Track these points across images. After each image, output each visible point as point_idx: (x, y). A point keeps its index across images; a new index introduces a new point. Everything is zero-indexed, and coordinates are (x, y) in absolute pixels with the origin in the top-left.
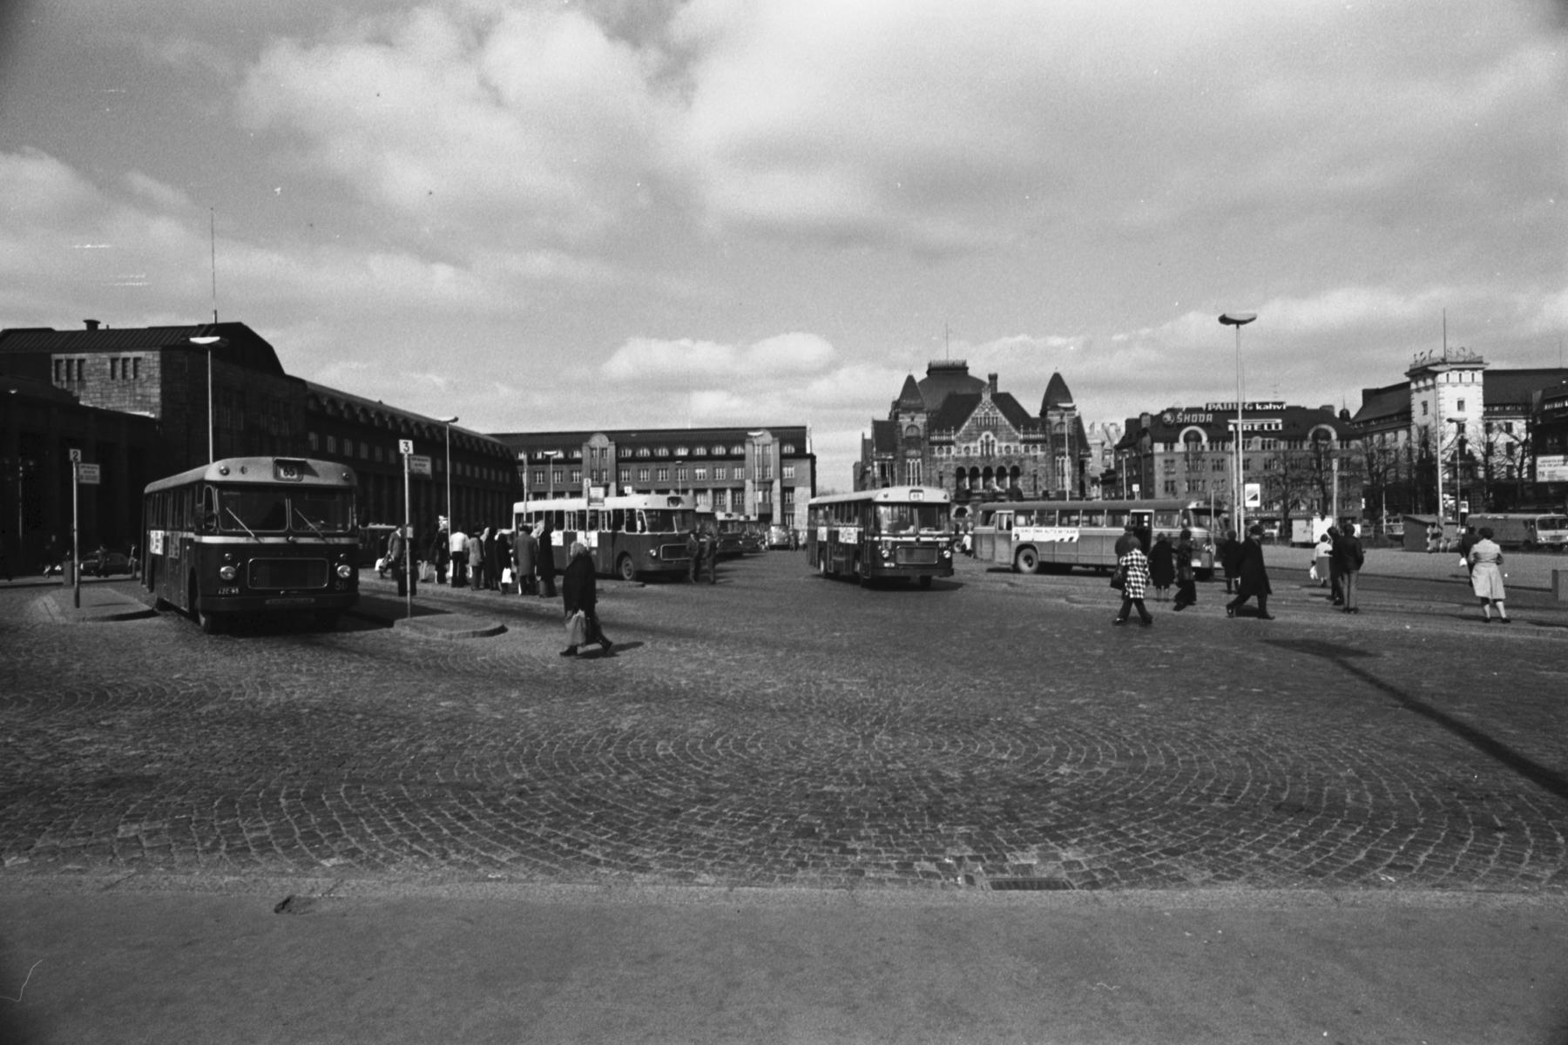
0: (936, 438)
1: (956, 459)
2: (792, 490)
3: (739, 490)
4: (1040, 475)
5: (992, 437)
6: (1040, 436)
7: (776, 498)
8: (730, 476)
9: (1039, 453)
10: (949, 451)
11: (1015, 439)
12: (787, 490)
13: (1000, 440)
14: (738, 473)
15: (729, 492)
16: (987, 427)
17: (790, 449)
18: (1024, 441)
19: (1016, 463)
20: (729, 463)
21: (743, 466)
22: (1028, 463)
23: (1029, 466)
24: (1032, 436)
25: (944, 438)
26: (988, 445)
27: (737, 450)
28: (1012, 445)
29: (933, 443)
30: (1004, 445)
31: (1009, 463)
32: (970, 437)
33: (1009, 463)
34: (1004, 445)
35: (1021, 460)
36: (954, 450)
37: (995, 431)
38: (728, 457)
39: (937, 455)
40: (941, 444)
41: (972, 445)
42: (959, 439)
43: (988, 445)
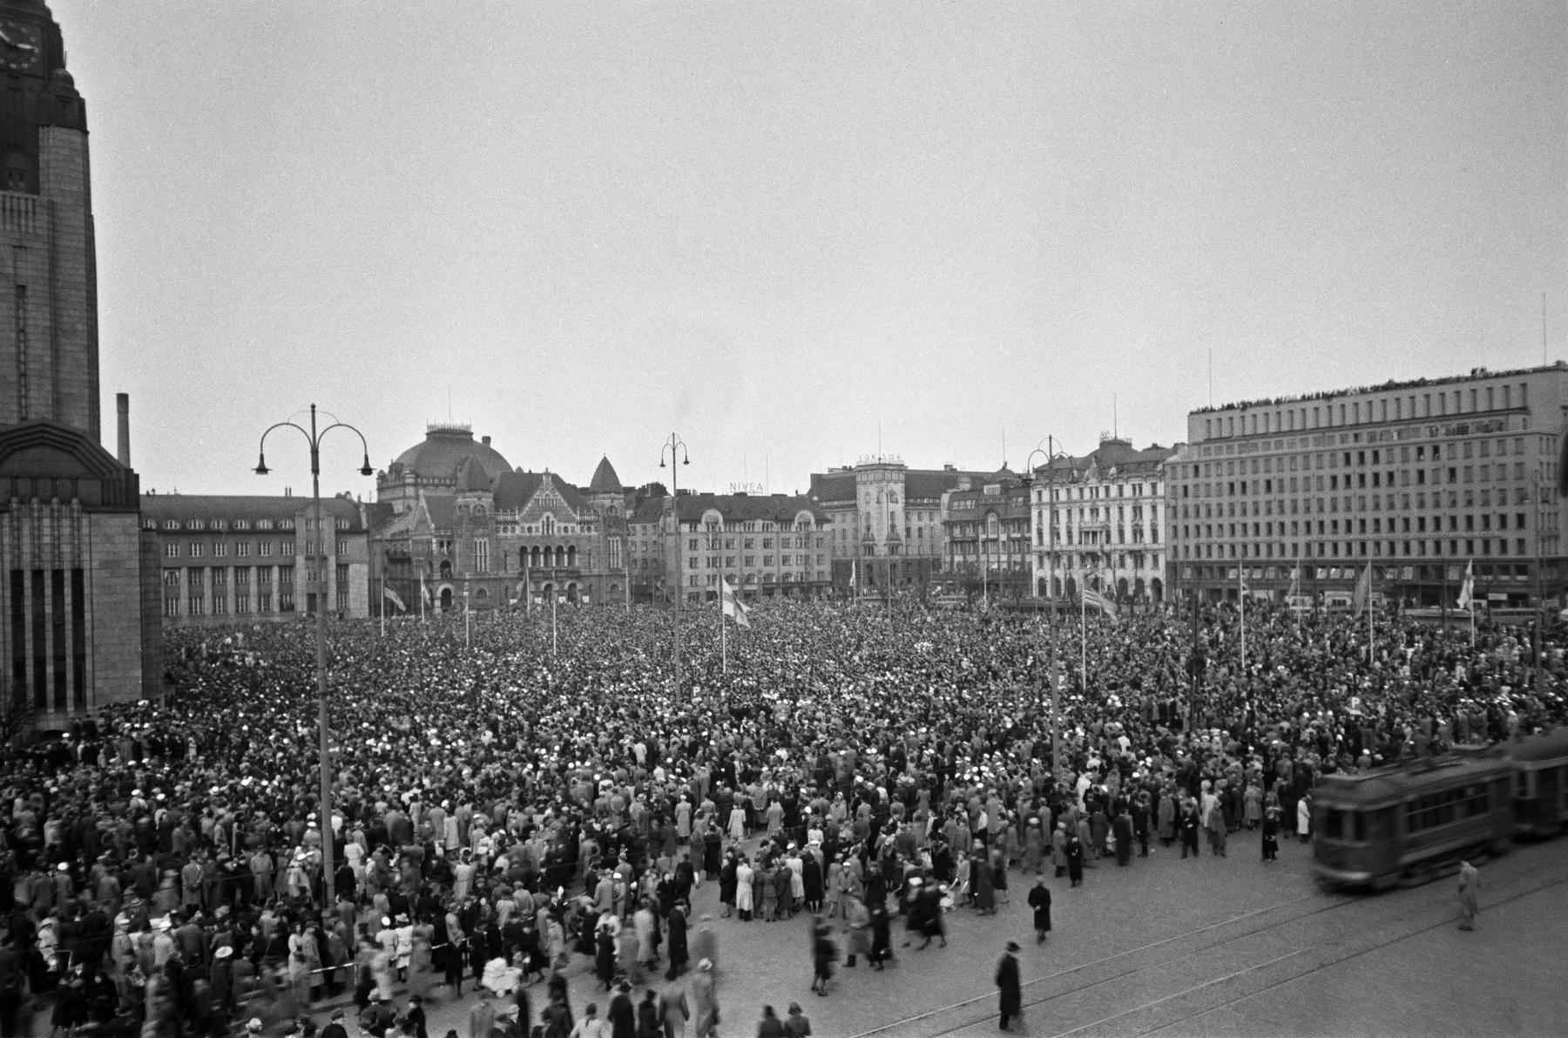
0: (501, 518)
1: (520, 538)
2: (346, 566)
3: (288, 568)
5: (552, 518)
7: (333, 576)
9: (593, 533)
10: (513, 530)
11: (573, 520)
12: (342, 567)
15: (276, 570)
17: (345, 525)
19: (573, 543)
22: (583, 542)
23: (584, 546)
24: (587, 518)
25: (509, 518)
26: (548, 524)
27: (287, 525)
28: (570, 526)
30: (563, 525)
34: (563, 525)
35: (578, 539)
38: (276, 531)
39: (502, 534)
40: (506, 523)
41: (534, 525)
43: (548, 524)
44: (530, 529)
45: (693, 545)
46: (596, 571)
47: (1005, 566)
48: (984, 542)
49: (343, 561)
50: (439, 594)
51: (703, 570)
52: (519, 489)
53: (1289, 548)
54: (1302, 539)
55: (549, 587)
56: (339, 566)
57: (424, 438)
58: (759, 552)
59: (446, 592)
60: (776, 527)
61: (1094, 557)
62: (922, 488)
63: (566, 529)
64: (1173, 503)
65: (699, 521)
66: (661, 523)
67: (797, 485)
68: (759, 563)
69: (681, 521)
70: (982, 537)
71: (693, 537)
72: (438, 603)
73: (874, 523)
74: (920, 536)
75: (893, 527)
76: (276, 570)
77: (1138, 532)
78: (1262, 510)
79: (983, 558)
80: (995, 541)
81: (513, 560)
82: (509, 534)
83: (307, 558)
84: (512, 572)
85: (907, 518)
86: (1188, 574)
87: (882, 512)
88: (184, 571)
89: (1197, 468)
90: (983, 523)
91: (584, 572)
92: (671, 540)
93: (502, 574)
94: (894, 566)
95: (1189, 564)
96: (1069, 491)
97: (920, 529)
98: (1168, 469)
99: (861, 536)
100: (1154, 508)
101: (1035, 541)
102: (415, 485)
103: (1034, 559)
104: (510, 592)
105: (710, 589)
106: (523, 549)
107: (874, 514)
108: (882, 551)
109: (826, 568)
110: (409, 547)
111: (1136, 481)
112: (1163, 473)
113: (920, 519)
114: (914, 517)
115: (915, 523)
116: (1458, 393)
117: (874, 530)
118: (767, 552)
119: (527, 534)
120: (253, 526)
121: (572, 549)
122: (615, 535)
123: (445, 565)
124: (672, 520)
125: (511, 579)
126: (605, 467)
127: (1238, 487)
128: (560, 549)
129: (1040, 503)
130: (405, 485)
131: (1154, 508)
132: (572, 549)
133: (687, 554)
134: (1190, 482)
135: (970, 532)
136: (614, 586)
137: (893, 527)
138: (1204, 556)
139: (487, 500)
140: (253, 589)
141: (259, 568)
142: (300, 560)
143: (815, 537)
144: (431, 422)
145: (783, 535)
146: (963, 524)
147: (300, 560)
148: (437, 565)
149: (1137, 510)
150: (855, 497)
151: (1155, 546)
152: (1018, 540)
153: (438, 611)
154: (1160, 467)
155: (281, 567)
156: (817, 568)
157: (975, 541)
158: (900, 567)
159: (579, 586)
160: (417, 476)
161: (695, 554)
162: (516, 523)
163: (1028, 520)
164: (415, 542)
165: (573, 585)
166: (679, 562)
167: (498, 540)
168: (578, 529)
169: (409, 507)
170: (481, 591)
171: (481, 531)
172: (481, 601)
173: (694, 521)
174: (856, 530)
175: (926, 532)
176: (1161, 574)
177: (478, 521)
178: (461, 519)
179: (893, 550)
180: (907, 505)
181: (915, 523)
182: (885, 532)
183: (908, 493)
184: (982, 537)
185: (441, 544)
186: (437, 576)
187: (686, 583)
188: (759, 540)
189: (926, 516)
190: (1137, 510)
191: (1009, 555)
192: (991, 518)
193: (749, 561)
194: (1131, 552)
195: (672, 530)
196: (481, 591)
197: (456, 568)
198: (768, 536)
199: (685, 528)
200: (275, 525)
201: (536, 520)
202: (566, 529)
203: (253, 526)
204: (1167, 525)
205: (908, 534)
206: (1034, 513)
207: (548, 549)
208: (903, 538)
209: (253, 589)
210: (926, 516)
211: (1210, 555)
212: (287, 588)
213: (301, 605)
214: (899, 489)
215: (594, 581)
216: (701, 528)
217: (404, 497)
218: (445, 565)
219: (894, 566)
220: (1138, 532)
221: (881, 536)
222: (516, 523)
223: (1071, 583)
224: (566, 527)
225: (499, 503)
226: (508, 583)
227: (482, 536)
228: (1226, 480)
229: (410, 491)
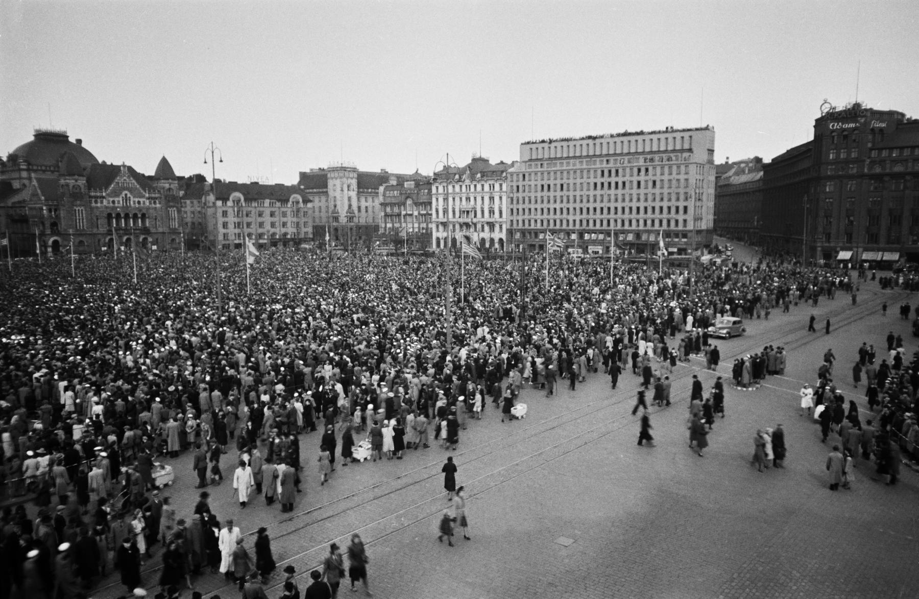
0: (93, 194)
1: (106, 207)
4: (159, 218)
5: (129, 195)
6: (157, 195)
9: (158, 205)
10: (102, 202)
11: (143, 197)
16: (125, 189)
18: (149, 198)
19: (144, 211)
24: (153, 195)
25: (98, 194)
26: (126, 199)
28: (141, 200)
29: (91, 197)
32: (116, 193)
34: (137, 200)
35: (148, 209)
37: (130, 190)
39: (93, 204)
40: (96, 197)
41: (116, 199)
42: (108, 195)
43: (126, 199)
44: (113, 202)
45: (225, 214)
46: (160, 230)
47: (416, 230)
48: (405, 216)
51: (232, 230)
52: (106, 175)
53: (571, 222)
54: (578, 218)
55: (128, 240)
57: (32, 138)
58: (267, 219)
59: (55, 242)
60: (278, 204)
61: (467, 225)
62: (368, 183)
63: (139, 202)
64: (511, 195)
65: (228, 199)
67: (291, 180)
68: (268, 226)
69: (217, 199)
70: (403, 213)
71: (224, 209)
72: (50, 249)
73: (338, 203)
74: (367, 211)
75: (350, 206)
77: (492, 212)
78: (558, 201)
79: (404, 225)
80: (411, 215)
81: (102, 222)
82: (99, 205)
84: (103, 229)
85: (359, 200)
86: (518, 236)
87: (343, 197)
89: (524, 176)
90: (404, 204)
91: (153, 230)
92: (210, 211)
93: (95, 231)
95: (519, 230)
96: (454, 187)
98: (509, 176)
99: (330, 211)
100: (501, 198)
101: (434, 216)
102: (28, 170)
103: (433, 226)
105: (237, 242)
106: (109, 216)
107: (338, 197)
108: (343, 220)
109: (310, 230)
111: (491, 182)
112: (506, 178)
113: (366, 201)
114: (363, 200)
115: (363, 204)
116: (667, 139)
117: (338, 207)
118: (273, 219)
119: (111, 205)
122: (173, 207)
123: (54, 225)
124: (211, 198)
125: (103, 234)
126: (164, 165)
127: (546, 187)
129: (437, 194)
130: (20, 170)
131: (501, 198)
133: (221, 220)
134: (521, 184)
135: (396, 210)
136: (173, 240)
137: (350, 206)
138: (527, 226)
139: (82, 182)
144: (37, 128)
145: (283, 209)
146: (392, 205)
148: (48, 225)
149: (492, 199)
150: (326, 187)
151: (501, 220)
152: (425, 215)
154: (504, 174)
156: (304, 230)
157: (399, 215)
159: (150, 239)
160: (29, 164)
161: (226, 219)
162: (104, 197)
163: (430, 203)
164: (31, 209)
165: (145, 239)
166: (216, 224)
167: (92, 209)
168: (147, 203)
169: (24, 185)
170: (81, 242)
171: (78, 202)
172: (81, 249)
173: (225, 199)
174: (327, 207)
175: (370, 210)
176: (503, 236)
177: (76, 196)
179: (351, 219)
182: (346, 208)
183: (360, 185)
184: (403, 213)
185: (50, 211)
186: (48, 232)
187: (221, 237)
188: (267, 212)
189: (370, 199)
190: (492, 199)
191: (419, 224)
192: (409, 202)
193: (261, 225)
194: (488, 223)
195: (211, 204)
196: (81, 242)
197: (63, 225)
198: (273, 209)
199: (219, 203)
201: (118, 196)
204: (507, 208)
206: (434, 200)
208: (356, 212)
210: (370, 199)
211: (530, 225)
214: (354, 183)
215: (160, 237)
216: (230, 203)
217: (20, 178)
220: (492, 212)
221: (343, 212)
222: (104, 197)
223: (454, 241)
224: (140, 201)
225: (90, 185)
226: (100, 237)
227: (80, 206)
228: (539, 183)
229: (24, 174)
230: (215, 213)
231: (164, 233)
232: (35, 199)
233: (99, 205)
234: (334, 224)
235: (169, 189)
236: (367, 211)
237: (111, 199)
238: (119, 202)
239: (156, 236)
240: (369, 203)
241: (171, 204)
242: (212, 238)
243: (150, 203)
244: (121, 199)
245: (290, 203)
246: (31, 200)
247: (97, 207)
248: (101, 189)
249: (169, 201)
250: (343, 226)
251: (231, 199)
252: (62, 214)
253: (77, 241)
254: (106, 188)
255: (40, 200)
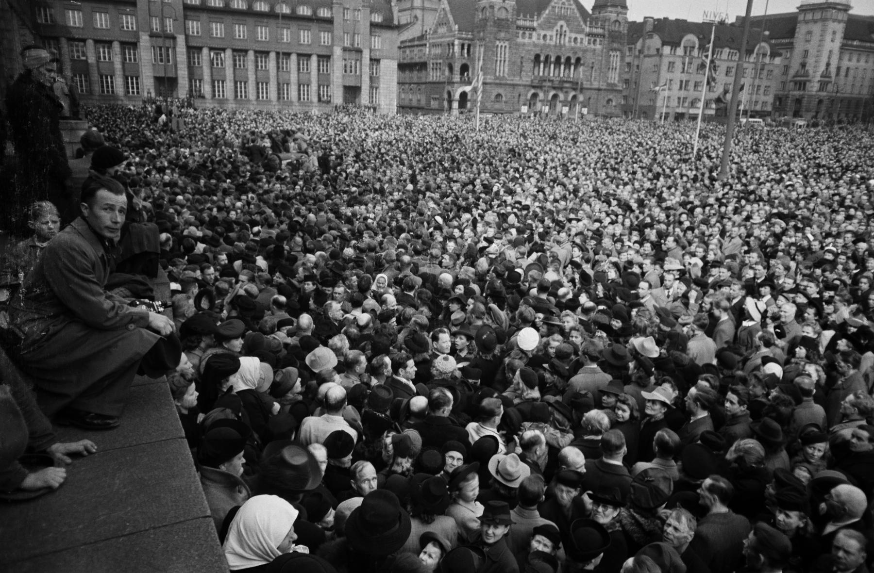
0: (521, 23)
1: (535, 45)
2: (378, 61)
3: (325, 58)
4: (596, 67)
5: (565, 28)
6: (600, 31)
7: (366, 70)
8: (316, 40)
9: (598, 47)
10: (530, 38)
11: (581, 31)
13: (571, 31)
14: (325, 37)
15: (314, 59)
16: (561, 17)
17: (378, 18)
18: (588, 35)
19: (580, 55)
20: (251, 21)
21: (331, 31)
22: (589, 55)
23: (588, 59)
24: (595, 31)
25: (528, 24)
26: (561, 34)
27: (324, 13)
28: (579, 36)
29: (519, 28)
31: (575, 53)
32: (549, 24)
33: (575, 53)
34: (573, 35)
35: (585, 51)
36: (534, 38)
39: (520, 40)
40: (525, 28)
41: (549, 33)
44: (545, 36)
45: (671, 64)
46: (596, 85)
49: (377, 55)
50: (457, 96)
51: (676, 92)
56: (371, 59)
59: (464, 95)
63: (576, 39)
65: (678, 45)
66: (639, 45)
69: (664, 44)
71: (671, 59)
72: (455, 105)
73: (811, 61)
74: (847, 75)
75: (828, 65)
76: (314, 59)
81: (528, 66)
82: (527, 40)
83: (345, 49)
84: (526, 79)
85: (840, 59)
88: (229, 52)
91: (586, 85)
93: (517, 80)
94: (820, 102)
97: (848, 69)
99: (792, 72)
104: (522, 98)
105: (680, 110)
106: (537, 57)
107: (812, 51)
108: (814, 87)
109: (770, 99)
110: (427, 52)
113: (850, 60)
114: (846, 57)
117: (810, 68)
119: (542, 41)
120: (294, 11)
121: (578, 60)
122: (615, 50)
123: (464, 68)
125: (525, 86)
128: (568, 59)
132: (578, 60)
133: (665, 75)
136: (609, 100)
137: (828, 65)
140: (294, 77)
141: (299, 55)
142: (338, 52)
143: (767, 68)
147: (338, 52)
148: (457, 68)
153: (455, 112)
155: (319, 56)
156: (763, 98)
158: (826, 102)
159: (581, 98)
162: (534, 29)
164: (434, 45)
165: (555, 96)
167: (518, 45)
168: (586, 40)
169: (416, 17)
171: (502, 35)
173: (675, 45)
174: (787, 68)
175: (851, 72)
177: (501, 25)
178: (486, 20)
179: (823, 85)
180: (843, 48)
181: (846, 63)
182: (822, 68)
183: (847, 36)
185: (463, 46)
186: (457, 78)
187: (659, 103)
189: (854, 59)
195: (653, 52)
196: (499, 95)
198: (731, 64)
199: (667, 50)
200: (315, 12)
201: (551, 28)
202: (576, 39)
203: (294, 11)
205: (838, 74)
207: (558, 58)
208: (833, 75)
209: (294, 77)
210: (854, 59)
212: (324, 81)
213: (338, 99)
214: (840, 28)
215: (593, 94)
216: (680, 51)
218: (464, 68)
219: (820, 102)
221: (816, 74)
222: (534, 29)
227: (504, 40)
230: (658, 67)
231: (599, 90)
232: (442, 30)
233: (527, 40)
234: (797, 93)
235: (617, 21)
236: (847, 75)
237: (543, 33)
238: (551, 36)
239: (588, 93)
240: (853, 64)
241: (615, 45)
242: (643, 102)
243: (589, 43)
244: (554, 33)
245: (755, 55)
246: (435, 32)
247: (524, 45)
248: (532, 16)
249: (613, 41)
250: (810, 96)
251: (682, 45)
252: (479, 51)
253: (495, 93)
254: (539, 15)
255: (450, 30)
